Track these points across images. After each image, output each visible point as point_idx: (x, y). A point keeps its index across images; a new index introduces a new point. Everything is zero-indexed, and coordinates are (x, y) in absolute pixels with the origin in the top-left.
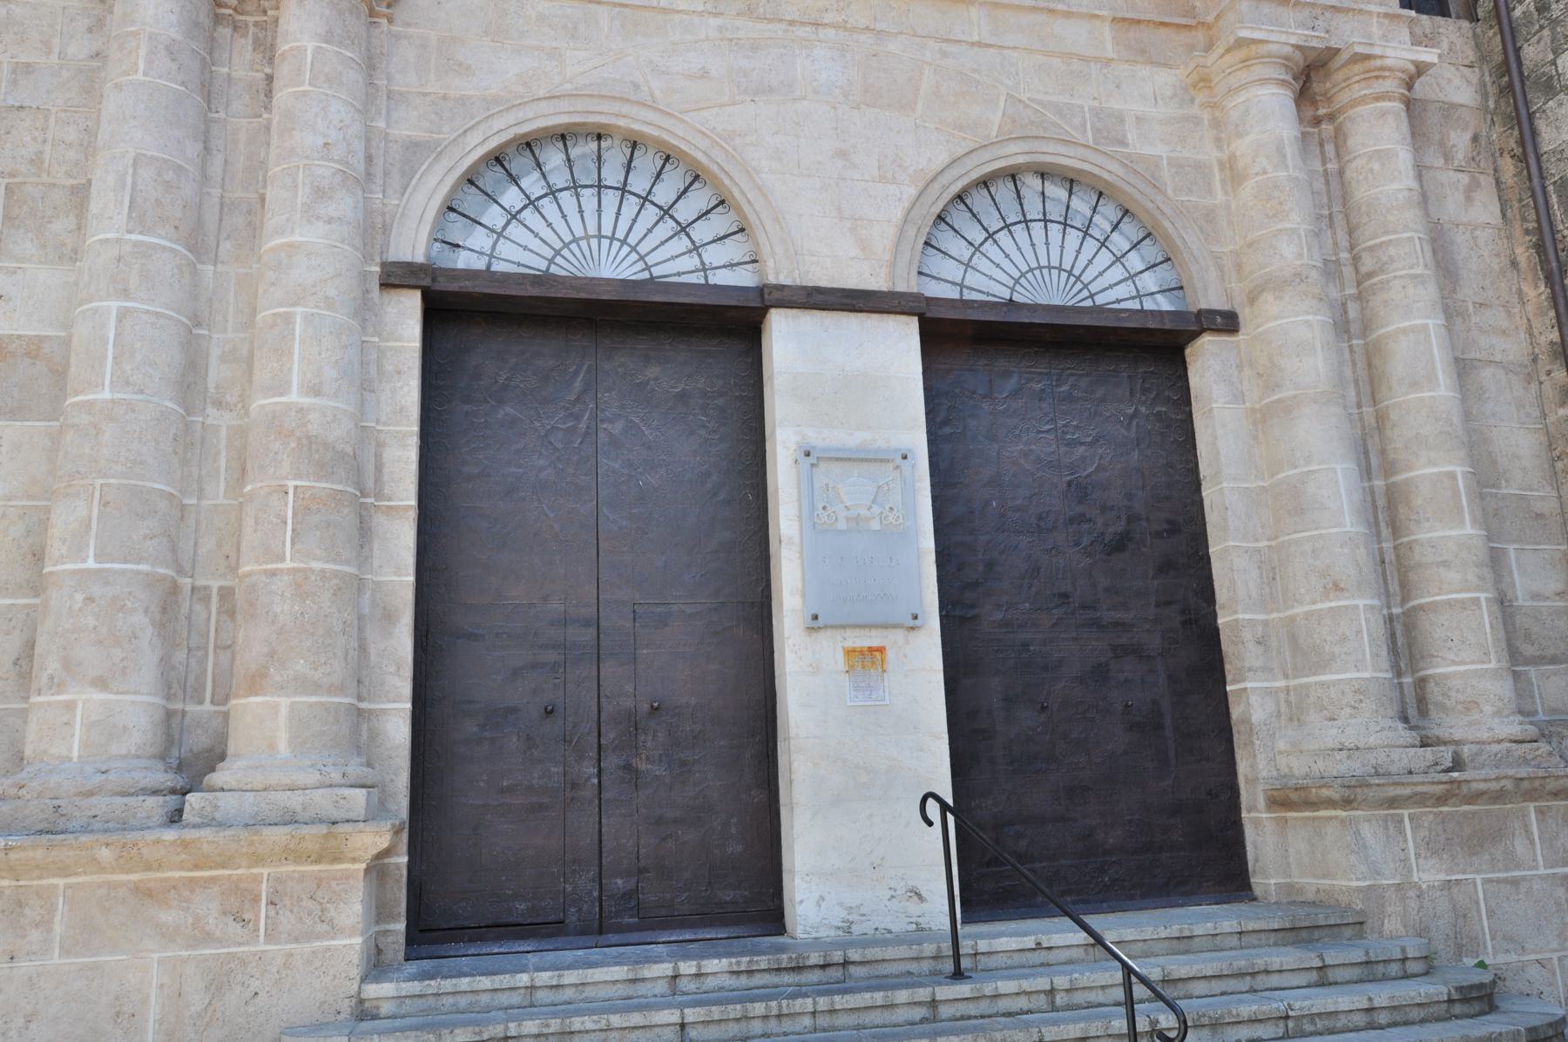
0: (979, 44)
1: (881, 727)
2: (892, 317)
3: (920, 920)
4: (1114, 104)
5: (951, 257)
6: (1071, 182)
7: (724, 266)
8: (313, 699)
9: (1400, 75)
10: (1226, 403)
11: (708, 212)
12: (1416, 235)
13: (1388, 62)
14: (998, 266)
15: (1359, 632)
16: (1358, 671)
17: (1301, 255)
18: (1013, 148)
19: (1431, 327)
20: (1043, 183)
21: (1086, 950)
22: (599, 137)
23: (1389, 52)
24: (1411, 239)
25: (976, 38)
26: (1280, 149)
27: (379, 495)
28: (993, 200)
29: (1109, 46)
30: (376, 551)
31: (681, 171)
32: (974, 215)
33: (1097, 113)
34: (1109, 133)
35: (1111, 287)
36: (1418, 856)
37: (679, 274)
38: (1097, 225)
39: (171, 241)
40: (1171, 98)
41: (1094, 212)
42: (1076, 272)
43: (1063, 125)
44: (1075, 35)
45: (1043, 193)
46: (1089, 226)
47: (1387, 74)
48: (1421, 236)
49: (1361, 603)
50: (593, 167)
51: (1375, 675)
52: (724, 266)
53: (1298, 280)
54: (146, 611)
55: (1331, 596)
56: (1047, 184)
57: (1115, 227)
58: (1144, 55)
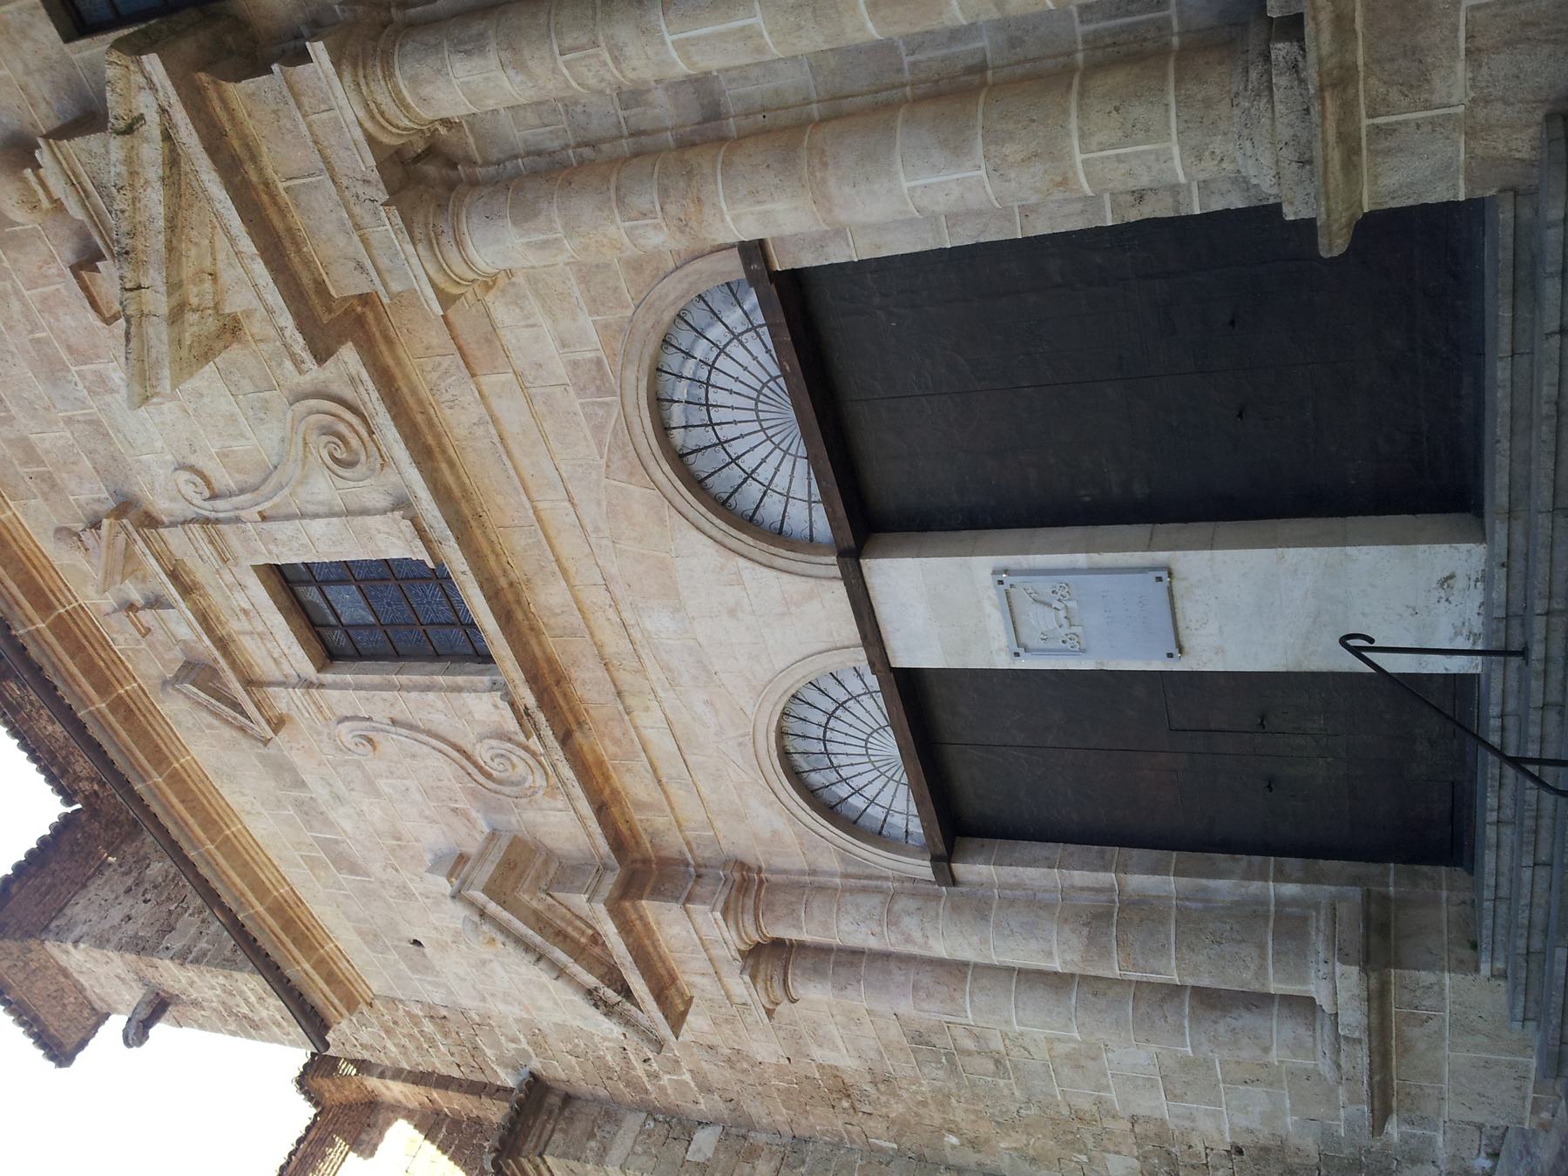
0: (570, 500)
1: (1272, 603)
2: (867, 580)
3: (1473, 578)
4: (561, 370)
5: (785, 511)
6: (658, 403)
7: (862, 681)
8: (1271, 970)
9: (364, 89)
10: (848, 245)
11: (819, 689)
12: (560, 60)
13: (362, 114)
14: (777, 469)
15: (1119, 159)
16: (1171, 159)
17: (656, 227)
18: (659, 477)
19: (675, 37)
20: (674, 428)
21: (1516, 519)
22: (788, 753)
23: (350, 117)
24: (567, 65)
25: (567, 504)
26: (543, 245)
27: (1111, 889)
28: (712, 474)
29: (503, 377)
30: (1154, 893)
31: (793, 707)
32: (736, 491)
33: (581, 390)
34: (595, 378)
35: (755, 358)
36: (1428, 106)
37: (880, 708)
38: (694, 373)
39: (964, 995)
40: (521, 308)
41: (681, 377)
42: (754, 395)
43: (613, 423)
44: (511, 412)
45: (685, 427)
46: (699, 381)
47: (372, 106)
48: (557, 52)
49: (1079, 157)
50: (812, 757)
51: (1174, 136)
52: (862, 681)
53: (688, 229)
54: (1216, 1022)
55: (1076, 187)
56: (674, 425)
57: (688, 355)
58: (491, 335)
